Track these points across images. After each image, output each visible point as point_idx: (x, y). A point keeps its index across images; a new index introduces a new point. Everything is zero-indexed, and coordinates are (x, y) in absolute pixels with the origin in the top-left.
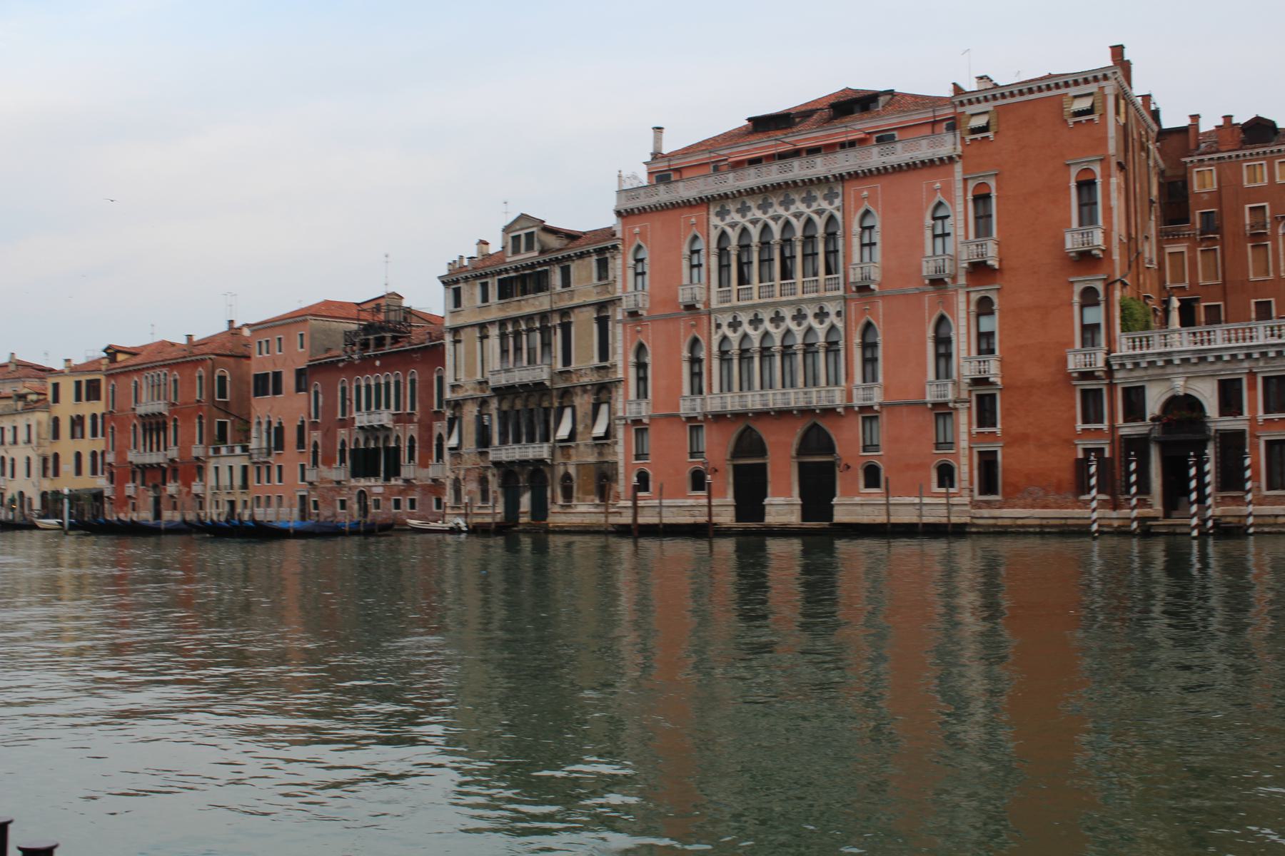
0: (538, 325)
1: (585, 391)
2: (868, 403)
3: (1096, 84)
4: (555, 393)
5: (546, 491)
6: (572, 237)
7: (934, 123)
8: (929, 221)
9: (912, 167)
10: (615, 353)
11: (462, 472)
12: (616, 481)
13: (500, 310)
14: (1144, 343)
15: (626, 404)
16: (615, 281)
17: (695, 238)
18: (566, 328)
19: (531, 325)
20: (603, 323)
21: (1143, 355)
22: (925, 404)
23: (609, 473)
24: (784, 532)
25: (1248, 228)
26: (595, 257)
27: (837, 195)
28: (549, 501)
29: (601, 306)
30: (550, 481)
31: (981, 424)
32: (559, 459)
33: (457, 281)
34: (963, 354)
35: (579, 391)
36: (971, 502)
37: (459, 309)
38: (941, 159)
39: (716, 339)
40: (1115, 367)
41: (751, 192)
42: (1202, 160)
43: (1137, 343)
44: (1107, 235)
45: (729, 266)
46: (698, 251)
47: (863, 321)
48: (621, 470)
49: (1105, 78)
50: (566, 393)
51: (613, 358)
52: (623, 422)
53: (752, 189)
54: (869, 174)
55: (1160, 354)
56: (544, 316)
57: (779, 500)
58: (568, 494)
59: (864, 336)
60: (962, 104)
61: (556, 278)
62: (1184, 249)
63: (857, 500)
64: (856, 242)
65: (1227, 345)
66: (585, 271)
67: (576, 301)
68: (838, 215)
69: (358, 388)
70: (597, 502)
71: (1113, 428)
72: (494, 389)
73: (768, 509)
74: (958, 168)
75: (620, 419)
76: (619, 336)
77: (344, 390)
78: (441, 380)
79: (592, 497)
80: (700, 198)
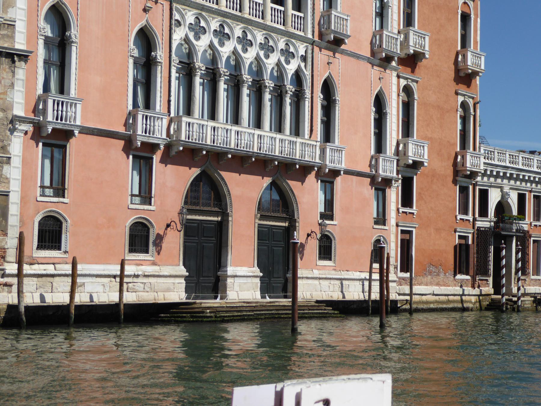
31: (404, 205)
48: (14, 209)
71: (475, 220)
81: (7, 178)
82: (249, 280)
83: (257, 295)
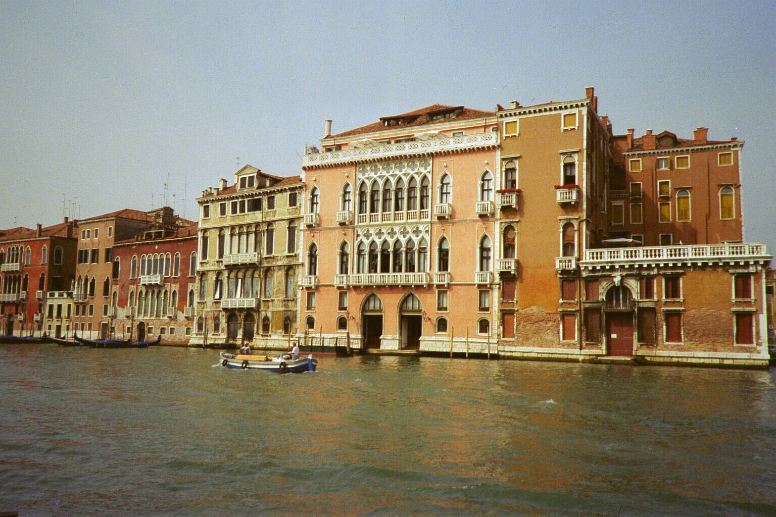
0: (254, 230)
1: (280, 269)
2: (442, 283)
3: (578, 109)
4: (262, 270)
5: (254, 325)
6: (275, 181)
7: (486, 127)
8: (480, 182)
9: (472, 151)
11: (204, 313)
12: (295, 321)
14: (599, 255)
15: (302, 278)
16: (300, 207)
17: (347, 185)
18: (270, 233)
19: (250, 229)
20: (292, 231)
21: (599, 263)
22: (474, 285)
23: (291, 317)
24: (391, 354)
25: (658, 194)
27: (429, 165)
28: (255, 332)
29: (291, 221)
30: (257, 321)
32: (262, 308)
33: (205, 202)
34: (497, 257)
35: (276, 269)
36: (498, 342)
37: (207, 218)
38: (488, 147)
39: (357, 242)
40: (583, 268)
41: (380, 160)
42: (635, 154)
43: (595, 256)
44: (579, 193)
45: (366, 201)
46: (349, 192)
47: (440, 236)
48: (298, 316)
49: (582, 105)
50: (268, 270)
52: (301, 288)
53: (381, 159)
54: (447, 154)
55: (607, 262)
56: (257, 225)
57: (389, 337)
58: (266, 328)
59: (440, 245)
60: (501, 116)
61: (265, 204)
62: (622, 204)
63: (434, 338)
64: (438, 191)
65: (645, 258)
66: (282, 200)
67: (277, 218)
68: (429, 176)
69: (143, 261)
70: (283, 334)
72: (226, 266)
73: (382, 341)
74: (498, 152)
75: (299, 286)
76: (301, 238)
77: (134, 262)
78: (194, 259)
79: (281, 331)
80: (351, 162)
82: (393, 341)
83: (397, 348)
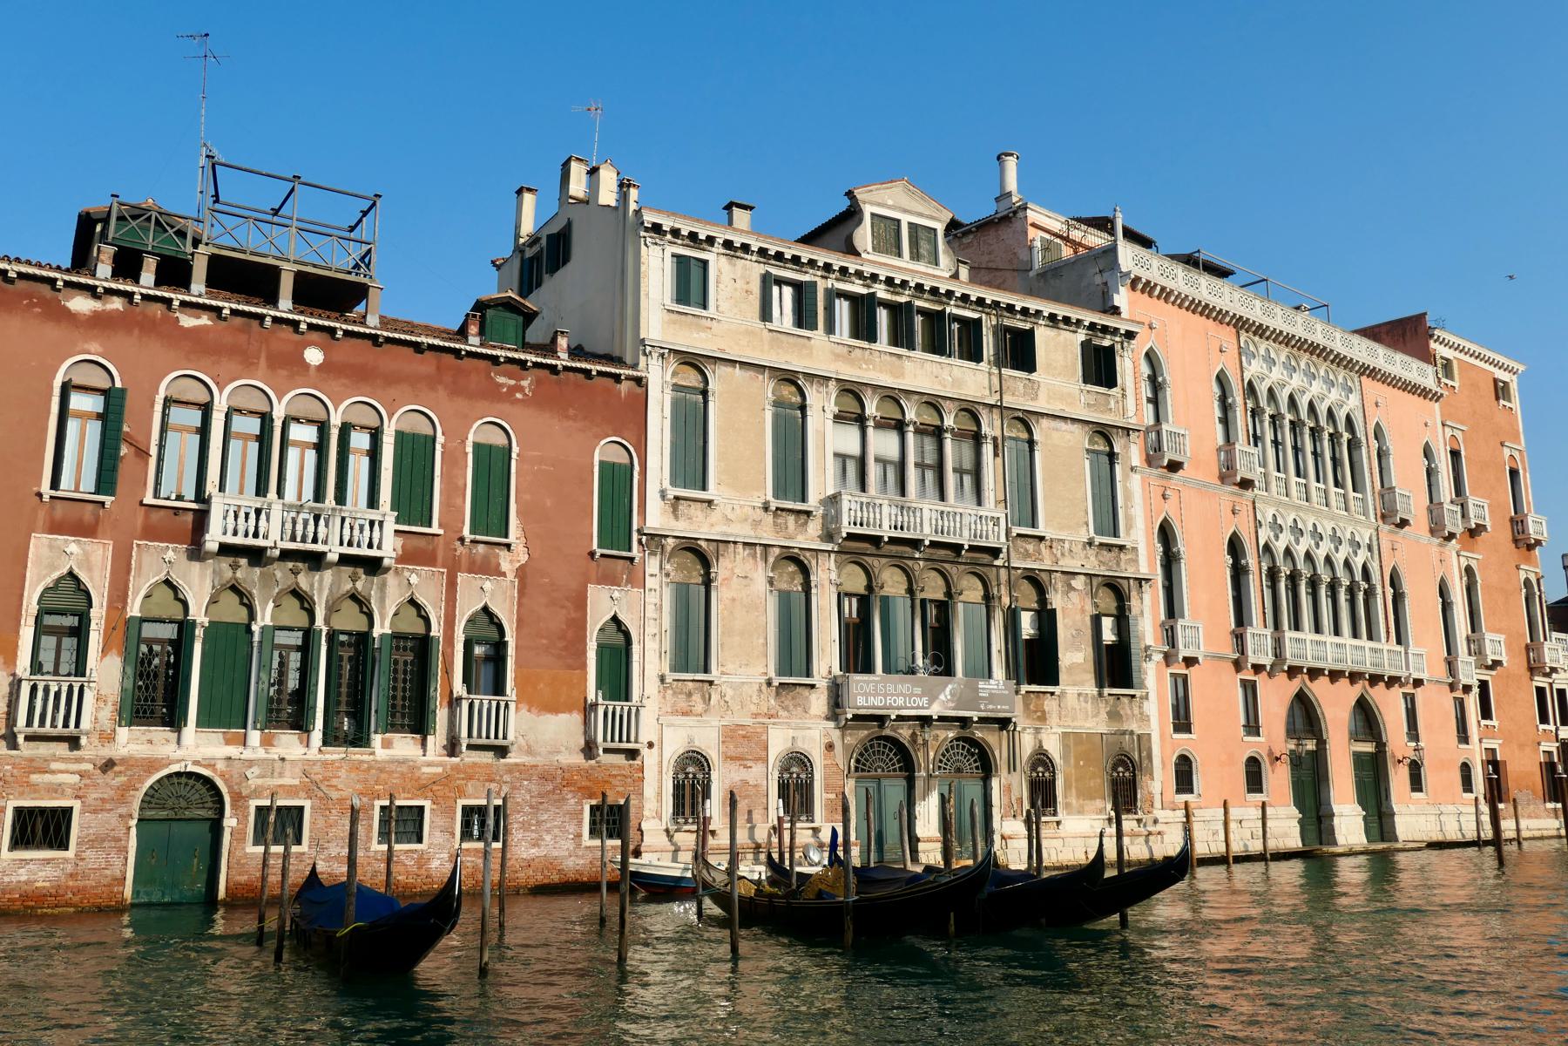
10: (1129, 528)
13: (837, 356)
26: (1082, 335)
51: (1128, 534)
67: (1040, 405)
79: (1099, 803)
81: (1148, 716)
